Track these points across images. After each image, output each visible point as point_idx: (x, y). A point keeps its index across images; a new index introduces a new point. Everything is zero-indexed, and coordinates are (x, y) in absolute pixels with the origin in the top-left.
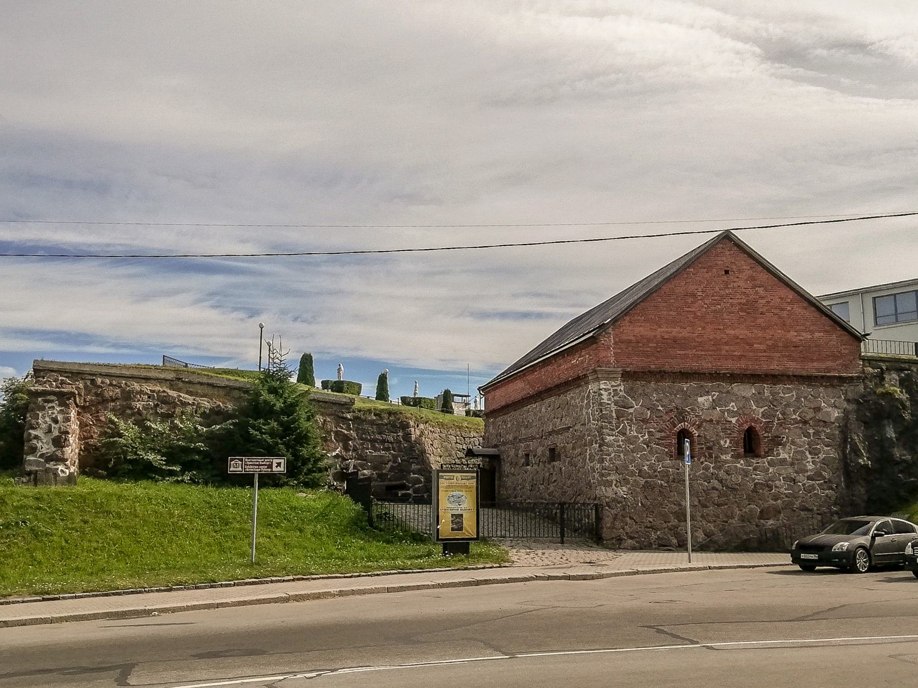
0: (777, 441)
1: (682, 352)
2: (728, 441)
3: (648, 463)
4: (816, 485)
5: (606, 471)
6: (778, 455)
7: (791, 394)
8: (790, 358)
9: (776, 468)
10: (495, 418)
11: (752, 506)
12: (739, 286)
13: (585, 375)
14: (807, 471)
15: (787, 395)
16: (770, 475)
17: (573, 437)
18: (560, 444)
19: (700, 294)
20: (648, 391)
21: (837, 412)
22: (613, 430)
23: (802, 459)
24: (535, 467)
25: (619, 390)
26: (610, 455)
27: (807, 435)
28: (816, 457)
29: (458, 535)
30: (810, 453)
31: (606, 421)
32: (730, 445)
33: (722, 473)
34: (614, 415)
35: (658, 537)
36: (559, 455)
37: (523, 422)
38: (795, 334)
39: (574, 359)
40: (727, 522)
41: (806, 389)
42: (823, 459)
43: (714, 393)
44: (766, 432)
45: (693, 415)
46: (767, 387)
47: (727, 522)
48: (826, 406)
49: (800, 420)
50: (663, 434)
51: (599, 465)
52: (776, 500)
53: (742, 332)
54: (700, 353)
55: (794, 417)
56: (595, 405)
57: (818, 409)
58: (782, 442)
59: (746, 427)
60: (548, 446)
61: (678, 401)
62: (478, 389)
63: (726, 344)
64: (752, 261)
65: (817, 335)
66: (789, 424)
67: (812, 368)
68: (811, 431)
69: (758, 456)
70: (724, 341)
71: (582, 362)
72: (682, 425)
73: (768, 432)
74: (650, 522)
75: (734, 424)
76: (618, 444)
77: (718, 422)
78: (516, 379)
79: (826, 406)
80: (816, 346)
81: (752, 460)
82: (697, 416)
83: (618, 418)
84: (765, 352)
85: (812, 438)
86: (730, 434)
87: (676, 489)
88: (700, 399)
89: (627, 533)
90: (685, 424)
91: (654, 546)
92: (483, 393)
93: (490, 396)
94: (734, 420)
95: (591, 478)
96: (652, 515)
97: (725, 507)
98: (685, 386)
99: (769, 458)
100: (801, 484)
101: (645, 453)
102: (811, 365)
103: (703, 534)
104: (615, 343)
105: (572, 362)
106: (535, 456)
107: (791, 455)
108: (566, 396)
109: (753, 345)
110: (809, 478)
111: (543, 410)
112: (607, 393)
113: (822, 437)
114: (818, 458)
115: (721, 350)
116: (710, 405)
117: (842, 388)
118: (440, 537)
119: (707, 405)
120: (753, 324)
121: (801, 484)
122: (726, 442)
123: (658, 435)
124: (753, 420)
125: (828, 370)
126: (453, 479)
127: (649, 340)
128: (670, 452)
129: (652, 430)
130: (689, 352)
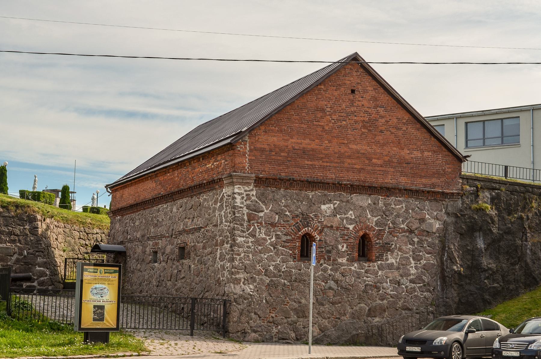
0: (386, 248)
1: (310, 163)
2: (345, 246)
3: (274, 263)
4: (417, 288)
5: (236, 270)
7: (401, 206)
8: (403, 174)
9: (384, 271)
10: (123, 216)
11: (362, 305)
12: (363, 105)
13: (220, 179)
14: (410, 275)
15: (397, 207)
16: (379, 278)
17: (204, 237)
18: (190, 243)
19: (329, 109)
20: (278, 197)
21: (438, 224)
22: (243, 232)
23: (407, 264)
24: (163, 264)
25: (251, 195)
26: (240, 255)
27: (412, 243)
28: (419, 263)
29: (99, 325)
30: (414, 259)
31: (238, 223)
33: (338, 275)
34: (246, 217)
35: (279, 331)
36: (189, 253)
37: (152, 220)
39: (209, 163)
40: (339, 319)
41: (414, 202)
42: (424, 265)
44: (378, 239)
45: (315, 221)
46: (381, 199)
47: (339, 319)
48: (430, 218)
49: (407, 229)
50: (289, 237)
51: (229, 264)
53: (363, 147)
54: (325, 164)
55: (402, 226)
56: (228, 208)
57: (422, 220)
58: (391, 248)
59: (361, 233)
60: (177, 244)
61: (303, 207)
62: (106, 187)
63: (349, 157)
64: (374, 83)
65: (426, 154)
66: (398, 233)
67: (420, 183)
68: (416, 240)
69: (369, 260)
71: (218, 167)
72: (306, 230)
73: (380, 239)
74: (272, 317)
75: (352, 231)
76: (248, 245)
77: (337, 228)
78: (147, 179)
79: (430, 218)
80: (425, 164)
81: (364, 264)
82: (319, 222)
83: (249, 221)
85: (416, 246)
86: (347, 240)
87: (297, 288)
88: (323, 207)
89: (251, 327)
90: (308, 229)
91: (274, 340)
92: (111, 191)
93: (118, 194)
94: (351, 227)
95: (220, 276)
96: (275, 311)
97: (339, 305)
98: (311, 194)
99: (379, 262)
100: (404, 286)
101: (272, 254)
102: (419, 181)
103: (318, 329)
104: (251, 150)
105: (208, 166)
106: (163, 254)
107: (398, 260)
108: (199, 198)
109: (372, 160)
110: (412, 281)
111: (175, 210)
112: (240, 197)
113: (425, 245)
114: (419, 264)
115: (343, 163)
116: (331, 212)
117: (444, 202)
118: (82, 327)
119: (329, 212)
121: (404, 286)
122: (343, 247)
123: (284, 238)
124: (367, 227)
125: (434, 185)
126: (97, 272)
127: (282, 151)
128: (294, 254)
129: (280, 233)
130: (316, 163)
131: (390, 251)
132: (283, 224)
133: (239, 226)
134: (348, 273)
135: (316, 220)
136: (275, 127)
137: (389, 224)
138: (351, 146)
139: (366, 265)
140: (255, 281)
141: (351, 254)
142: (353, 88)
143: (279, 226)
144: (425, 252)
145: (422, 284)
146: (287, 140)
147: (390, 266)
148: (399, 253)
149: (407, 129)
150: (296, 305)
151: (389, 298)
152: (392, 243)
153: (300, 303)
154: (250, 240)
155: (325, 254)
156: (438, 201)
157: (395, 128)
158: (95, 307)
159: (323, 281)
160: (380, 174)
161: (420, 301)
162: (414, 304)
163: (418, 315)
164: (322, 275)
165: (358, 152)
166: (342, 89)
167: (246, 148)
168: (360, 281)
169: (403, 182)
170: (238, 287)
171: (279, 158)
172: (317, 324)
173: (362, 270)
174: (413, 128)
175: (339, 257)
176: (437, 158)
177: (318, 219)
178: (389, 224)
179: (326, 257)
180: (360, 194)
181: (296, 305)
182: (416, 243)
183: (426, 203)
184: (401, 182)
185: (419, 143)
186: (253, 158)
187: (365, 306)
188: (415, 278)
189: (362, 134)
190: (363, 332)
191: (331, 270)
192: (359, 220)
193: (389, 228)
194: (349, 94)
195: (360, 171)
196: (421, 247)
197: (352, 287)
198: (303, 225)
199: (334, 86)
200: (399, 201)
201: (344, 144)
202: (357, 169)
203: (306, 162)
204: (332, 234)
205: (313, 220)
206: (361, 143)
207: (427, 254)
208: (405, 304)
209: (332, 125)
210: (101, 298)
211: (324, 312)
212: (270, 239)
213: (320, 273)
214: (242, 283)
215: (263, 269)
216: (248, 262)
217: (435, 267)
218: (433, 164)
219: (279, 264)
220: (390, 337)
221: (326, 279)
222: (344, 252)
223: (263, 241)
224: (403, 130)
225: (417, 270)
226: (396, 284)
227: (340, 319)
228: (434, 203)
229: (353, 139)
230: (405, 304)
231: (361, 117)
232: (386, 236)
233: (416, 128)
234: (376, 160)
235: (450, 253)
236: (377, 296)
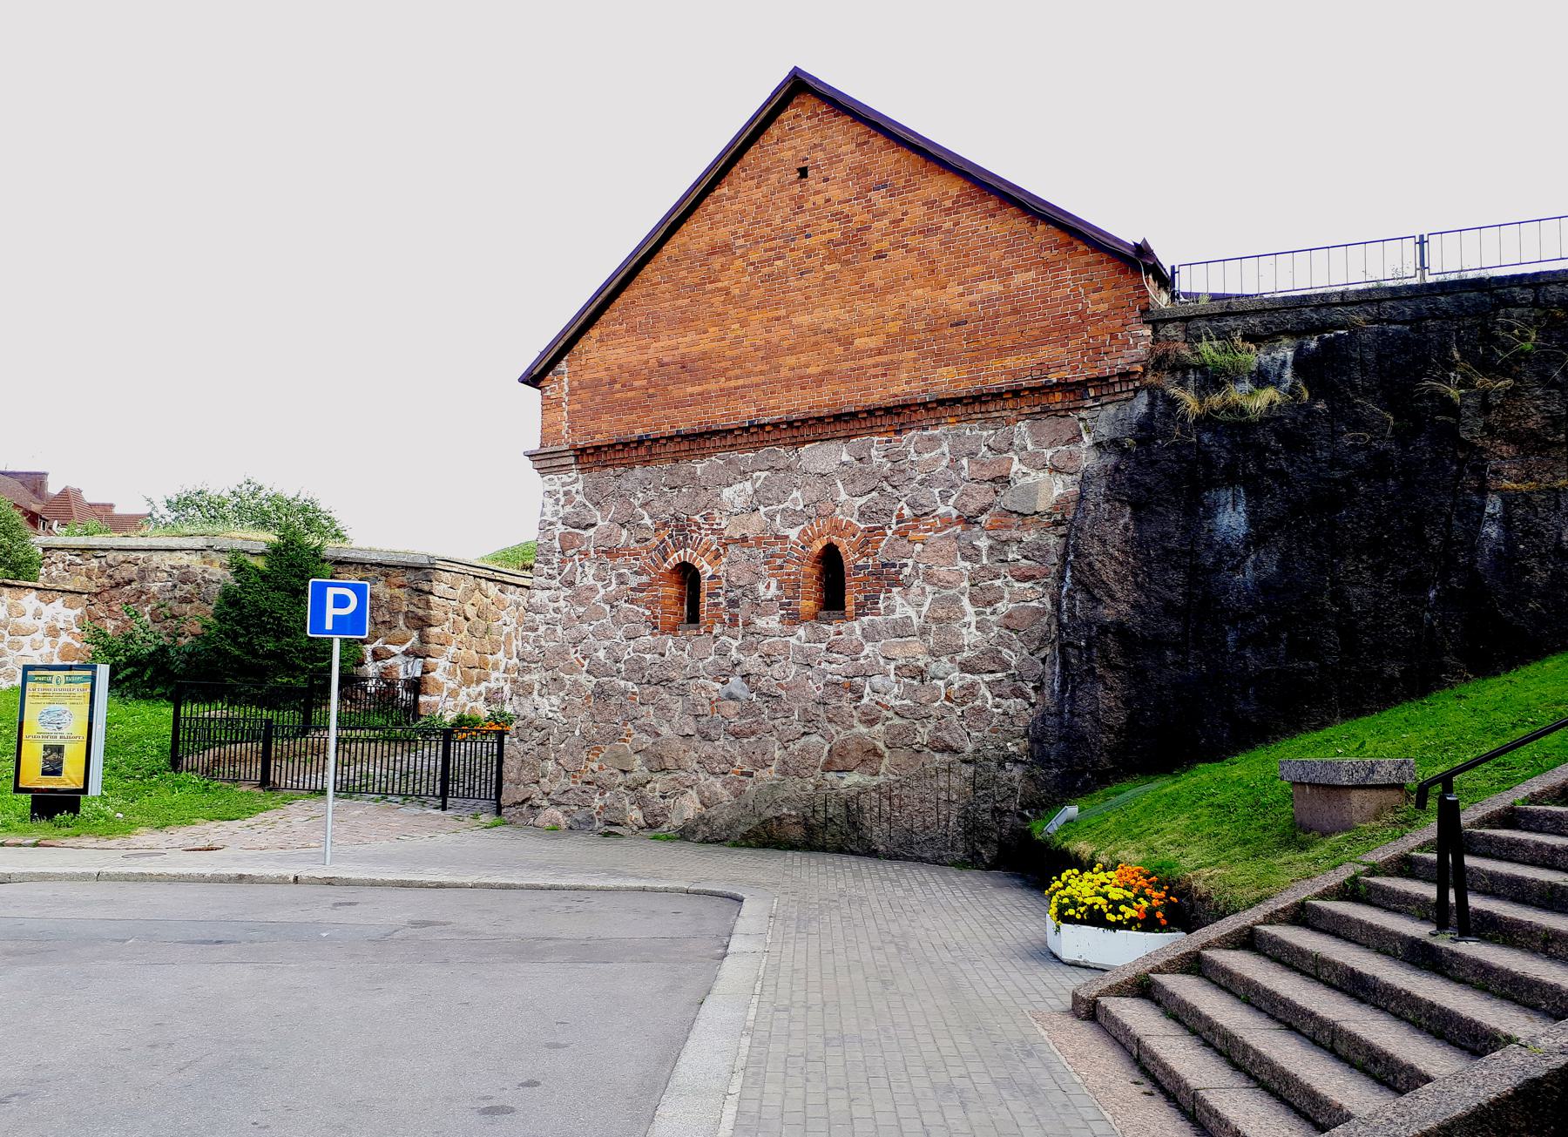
0: (887, 576)
2: (774, 584)
3: (607, 643)
5: (526, 664)
6: (890, 610)
7: (939, 451)
8: (940, 358)
9: (880, 643)
11: (814, 738)
12: (828, 201)
14: (960, 649)
15: (926, 456)
16: (862, 661)
19: (741, 242)
20: (629, 486)
21: (1061, 484)
22: (551, 577)
25: (574, 491)
26: (536, 630)
27: (972, 554)
28: (988, 610)
29: (51, 783)
31: (540, 558)
32: (778, 593)
33: (752, 662)
34: (557, 544)
38: (961, 289)
40: (750, 775)
42: (1009, 616)
43: (758, 473)
44: (863, 555)
45: (706, 530)
46: (879, 442)
47: (750, 775)
48: (1025, 469)
50: (645, 579)
52: (871, 722)
53: (830, 314)
54: (733, 383)
55: (942, 510)
58: (901, 577)
59: (818, 546)
61: (679, 502)
63: (792, 350)
64: (859, 128)
65: (1018, 279)
66: (930, 530)
67: (996, 375)
70: (785, 344)
73: (867, 556)
75: (795, 543)
76: (556, 605)
77: (759, 541)
79: (1025, 469)
80: (1015, 311)
81: (826, 627)
84: (880, 354)
85: (985, 561)
86: (781, 567)
87: (654, 698)
94: (793, 534)
96: (597, 755)
97: (753, 739)
98: (700, 467)
99: (865, 619)
101: (604, 621)
103: (697, 801)
104: (572, 392)
109: (852, 343)
110: (966, 667)
112: (552, 501)
113: (1010, 557)
115: (777, 369)
116: (746, 502)
117: (1083, 414)
119: (739, 502)
120: (857, 288)
122: (768, 587)
123: (634, 581)
124: (837, 529)
125: (1043, 367)
127: (634, 374)
129: (626, 571)
130: (712, 386)
131: (901, 585)
132: (635, 549)
133: (542, 565)
134: (781, 655)
135: (707, 526)
136: (621, 324)
137: (902, 508)
138: (797, 319)
139: (831, 629)
140: (562, 688)
141: (790, 604)
142: (802, 165)
143: (625, 555)
144: (1013, 576)
145: (999, 675)
146: (647, 347)
147: (901, 630)
148: (928, 588)
149: (956, 224)
150: (647, 741)
151: (891, 719)
152: (905, 561)
153: (658, 735)
154: (563, 595)
155: (724, 608)
156: (1063, 413)
157: (920, 232)
158: (45, 748)
159: (715, 679)
160: (877, 376)
161: (988, 725)
162: (968, 734)
163: (971, 769)
164: (715, 663)
165: (815, 331)
166: (774, 178)
167: (561, 388)
168: (810, 673)
169: (944, 383)
170: (527, 703)
171: (630, 394)
172: (695, 787)
173: (819, 645)
174: (977, 214)
175: (759, 615)
176: (1057, 282)
177: (713, 525)
178: (902, 508)
179: (726, 618)
180: (822, 440)
181: (647, 741)
182: (984, 552)
183: (1020, 427)
184: (936, 384)
185: (995, 255)
186: (578, 407)
187: (822, 741)
188: (978, 657)
189: (825, 279)
190: (793, 813)
191: (739, 649)
192: (818, 510)
193: (900, 519)
194: (790, 184)
195: (819, 380)
196: (1002, 561)
197: (787, 690)
198: (674, 545)
199: (752, 178)
201: (778, 319)
202: (813, 375)
203: (690, 390)
204: (745, 557)
205: (700, 528)
206: (823, 306)
207: (1017, 580)
208: (939, 734)
209: (748, 278)
210: (57, 731)
211: (711, 758)
212: (604, 587)
213: (711, 658)
214: (535, 693)
215: (584, 658)
216: (552, 644)
217: (1046, 618)
218: (1043, 302)
219: (618, 644)
220: (882, 830)
221: (725, 672)
222: (772, 600)
223: (588, 593)
224: (943, 233)
225: (983, 632)
226: (914, 678)
227: (752, 776)
228: (1048, 424)
229: (801, 298)
230: (939, 734)
231: (824, 233)
232: (886, 545)
233: (985, 212)
234: (863, 340)
235: (1082, 572)
236: (854, 713)
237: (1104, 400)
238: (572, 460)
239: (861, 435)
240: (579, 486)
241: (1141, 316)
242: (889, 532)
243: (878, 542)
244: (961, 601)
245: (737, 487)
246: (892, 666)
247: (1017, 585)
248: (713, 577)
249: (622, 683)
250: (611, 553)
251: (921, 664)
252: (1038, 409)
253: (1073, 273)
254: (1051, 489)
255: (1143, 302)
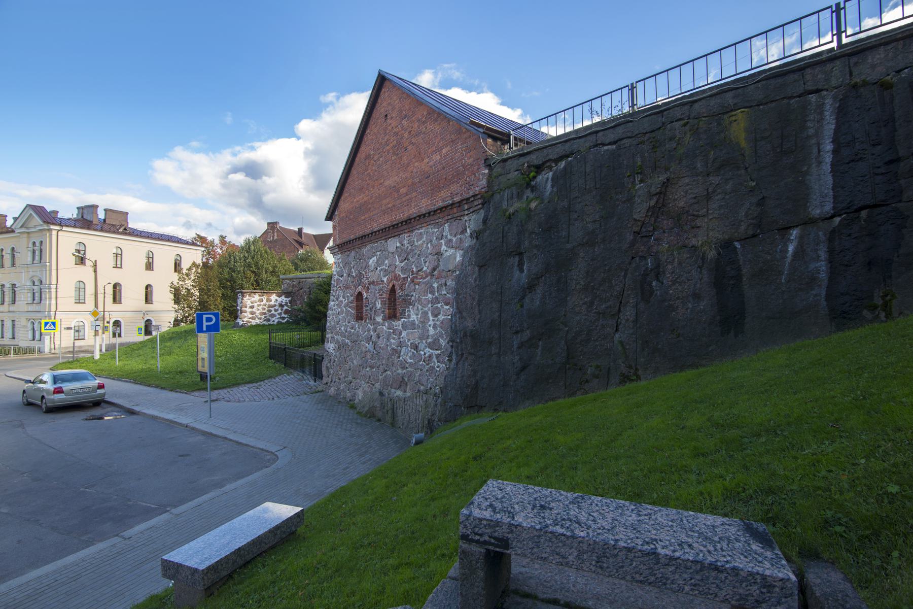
0: (408, 302)
4: (434, 357)
6: (409, 316)
11: (389, 373)
14: (428, 337)
15: (419, 243)
19: (372, 153)
27: (432, 293)
44: (402, 290)
68: (435, 285)
84: (406, 195)
99: (402, 320)
107: (419, 317)
117: (466, 218)
145: (439, 351)
156: (459, 218)
176: (456, 150)
200: (421, 233)
201: (381, 184)
237: (471, 210)
238: (337, 250)
239: (402, 234)
240: (341, 260)
241: (485, 162)
242: (409, 279)
243: (405, 284)
244: (428, 314)
245: (373, 259)
246: (409, 343)
247: (445, 307)
248: (366, 298)
249: (347, 341)
250: (346, 288)
251: (417, 343)
252: (450, 217)
253: (461, 145)
254: (455, 258)
255: (484, 155)
